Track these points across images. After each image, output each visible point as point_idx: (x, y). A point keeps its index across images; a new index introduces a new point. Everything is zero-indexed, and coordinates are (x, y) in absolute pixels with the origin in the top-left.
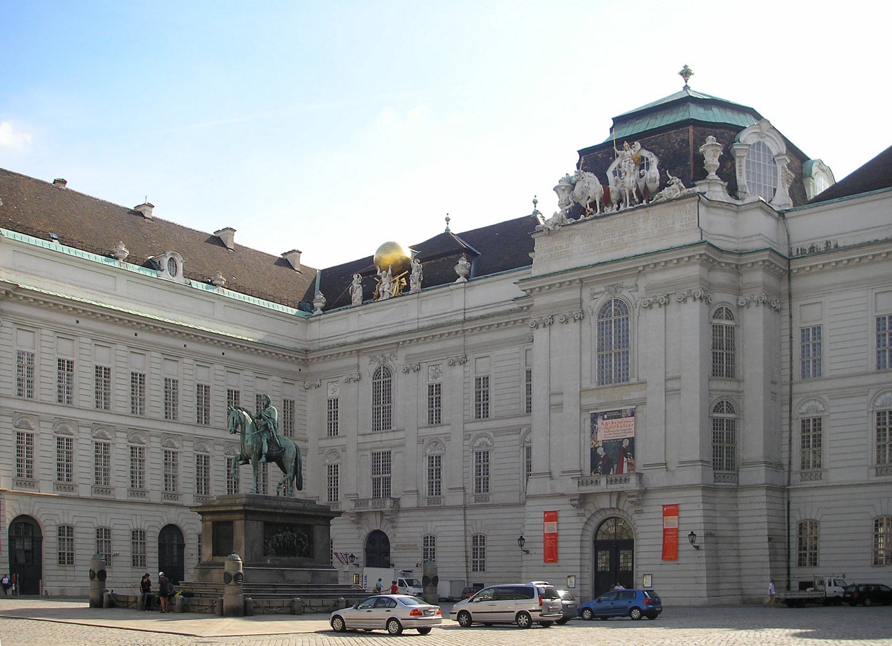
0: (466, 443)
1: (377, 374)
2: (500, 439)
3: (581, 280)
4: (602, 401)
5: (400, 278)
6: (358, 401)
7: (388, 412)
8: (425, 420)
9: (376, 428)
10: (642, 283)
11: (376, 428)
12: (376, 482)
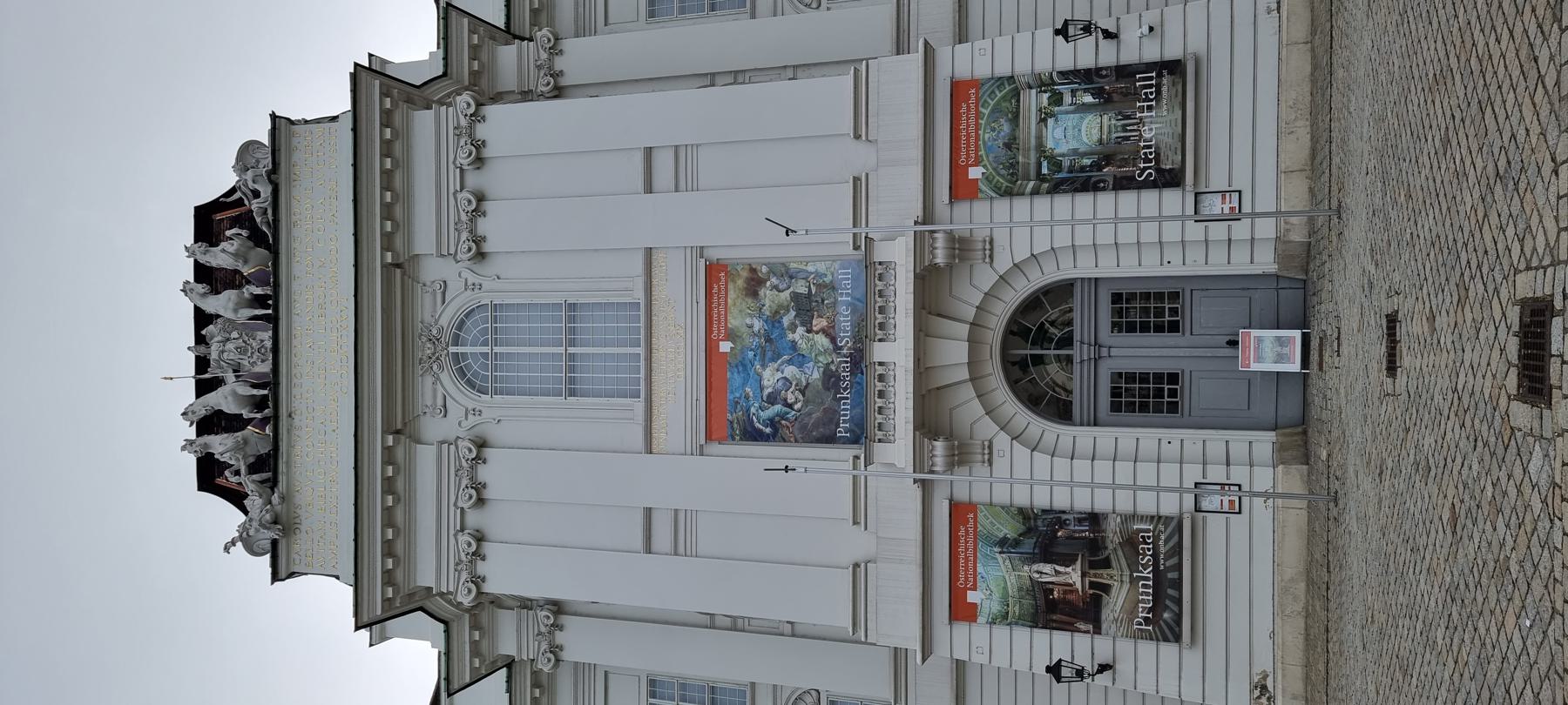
3: (389, 429)
10: (433, 270)
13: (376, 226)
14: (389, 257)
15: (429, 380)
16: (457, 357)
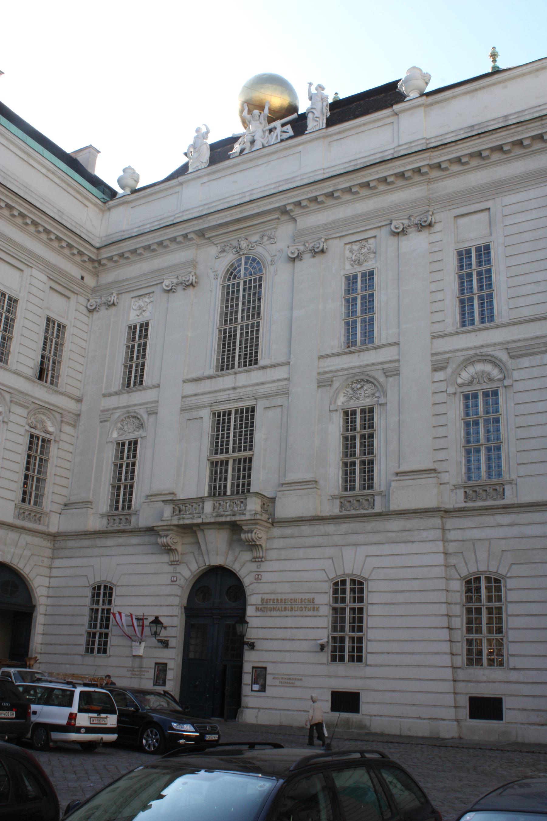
0: (440, 376)
1: (232, 273)
2: (526, 362)
5: (283, 125)
6: (187, 331)
7: (253, 334)
8: (336, 338)
9: (225, 364)
11: (225, 364)
12: (217, 469)
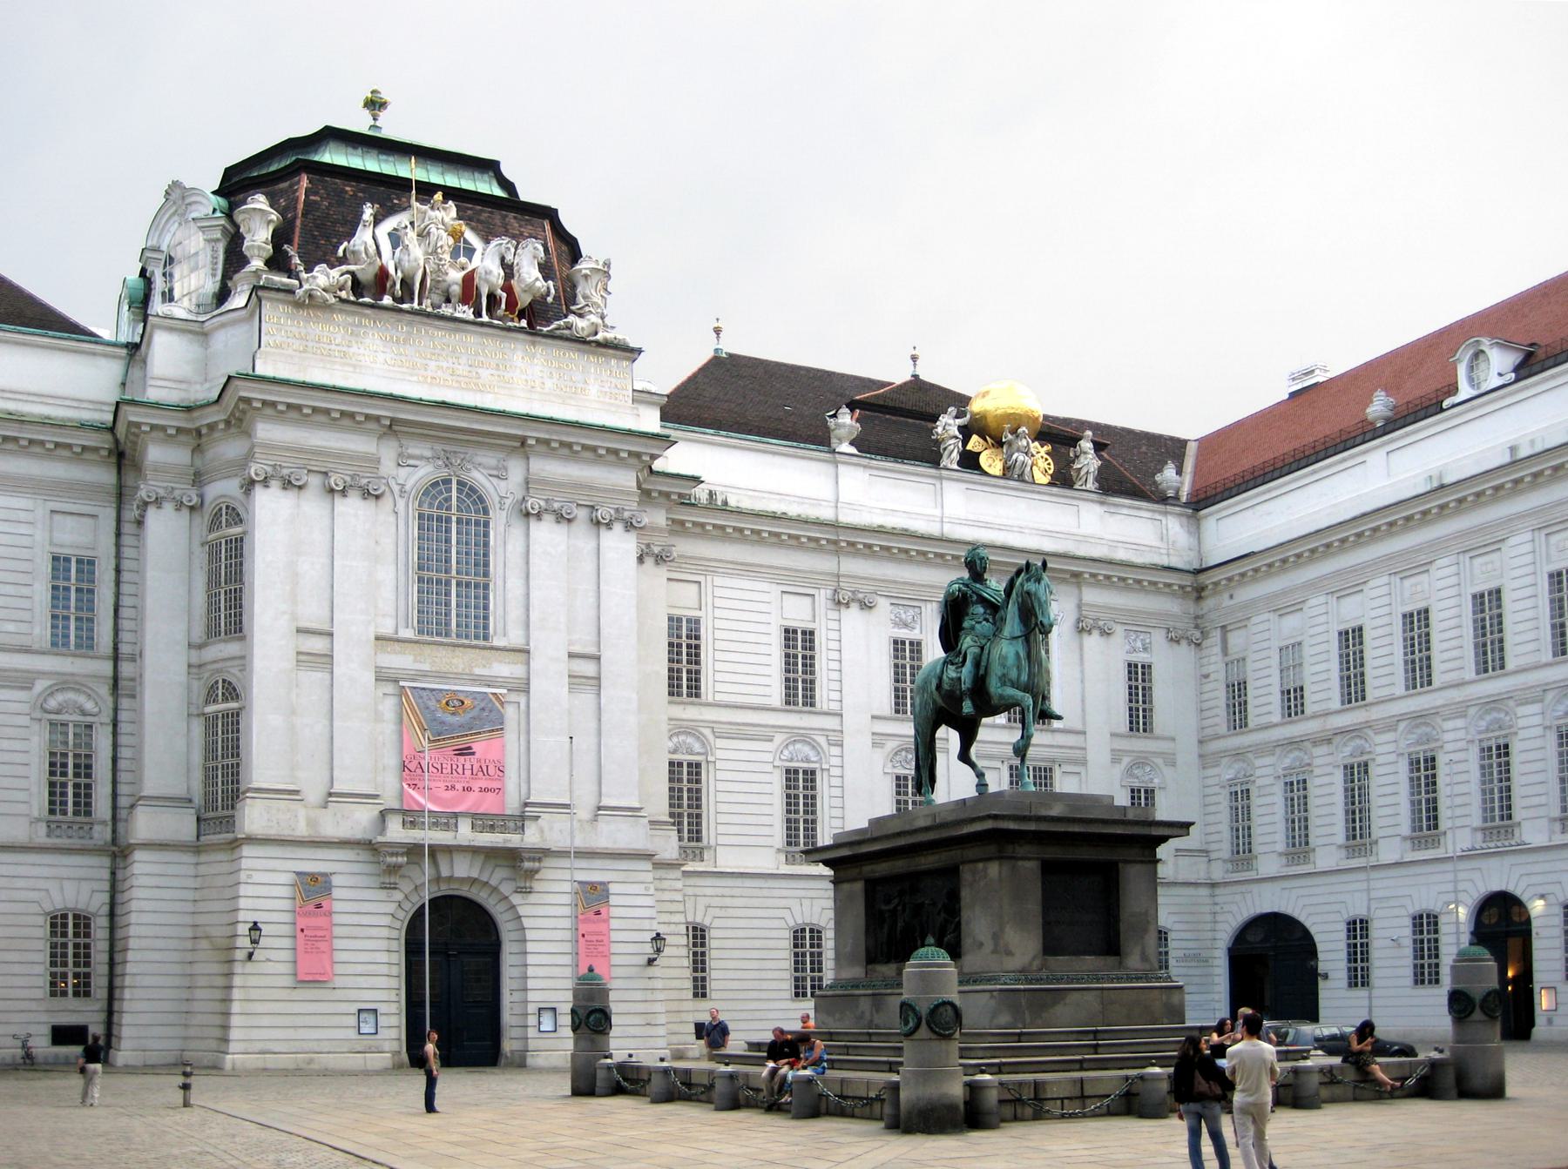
4: (426, 667)
13: (557, 435)
14: (531, 442)
15: (428, 454)
16: (449, 482)
